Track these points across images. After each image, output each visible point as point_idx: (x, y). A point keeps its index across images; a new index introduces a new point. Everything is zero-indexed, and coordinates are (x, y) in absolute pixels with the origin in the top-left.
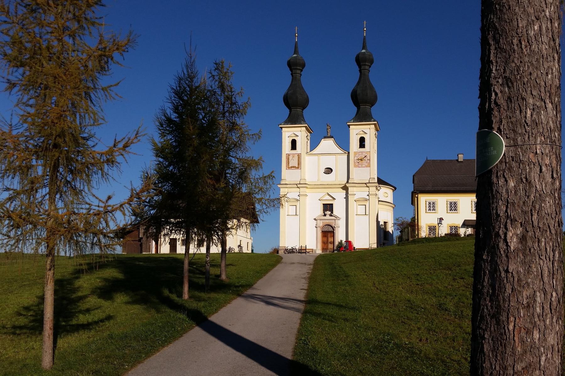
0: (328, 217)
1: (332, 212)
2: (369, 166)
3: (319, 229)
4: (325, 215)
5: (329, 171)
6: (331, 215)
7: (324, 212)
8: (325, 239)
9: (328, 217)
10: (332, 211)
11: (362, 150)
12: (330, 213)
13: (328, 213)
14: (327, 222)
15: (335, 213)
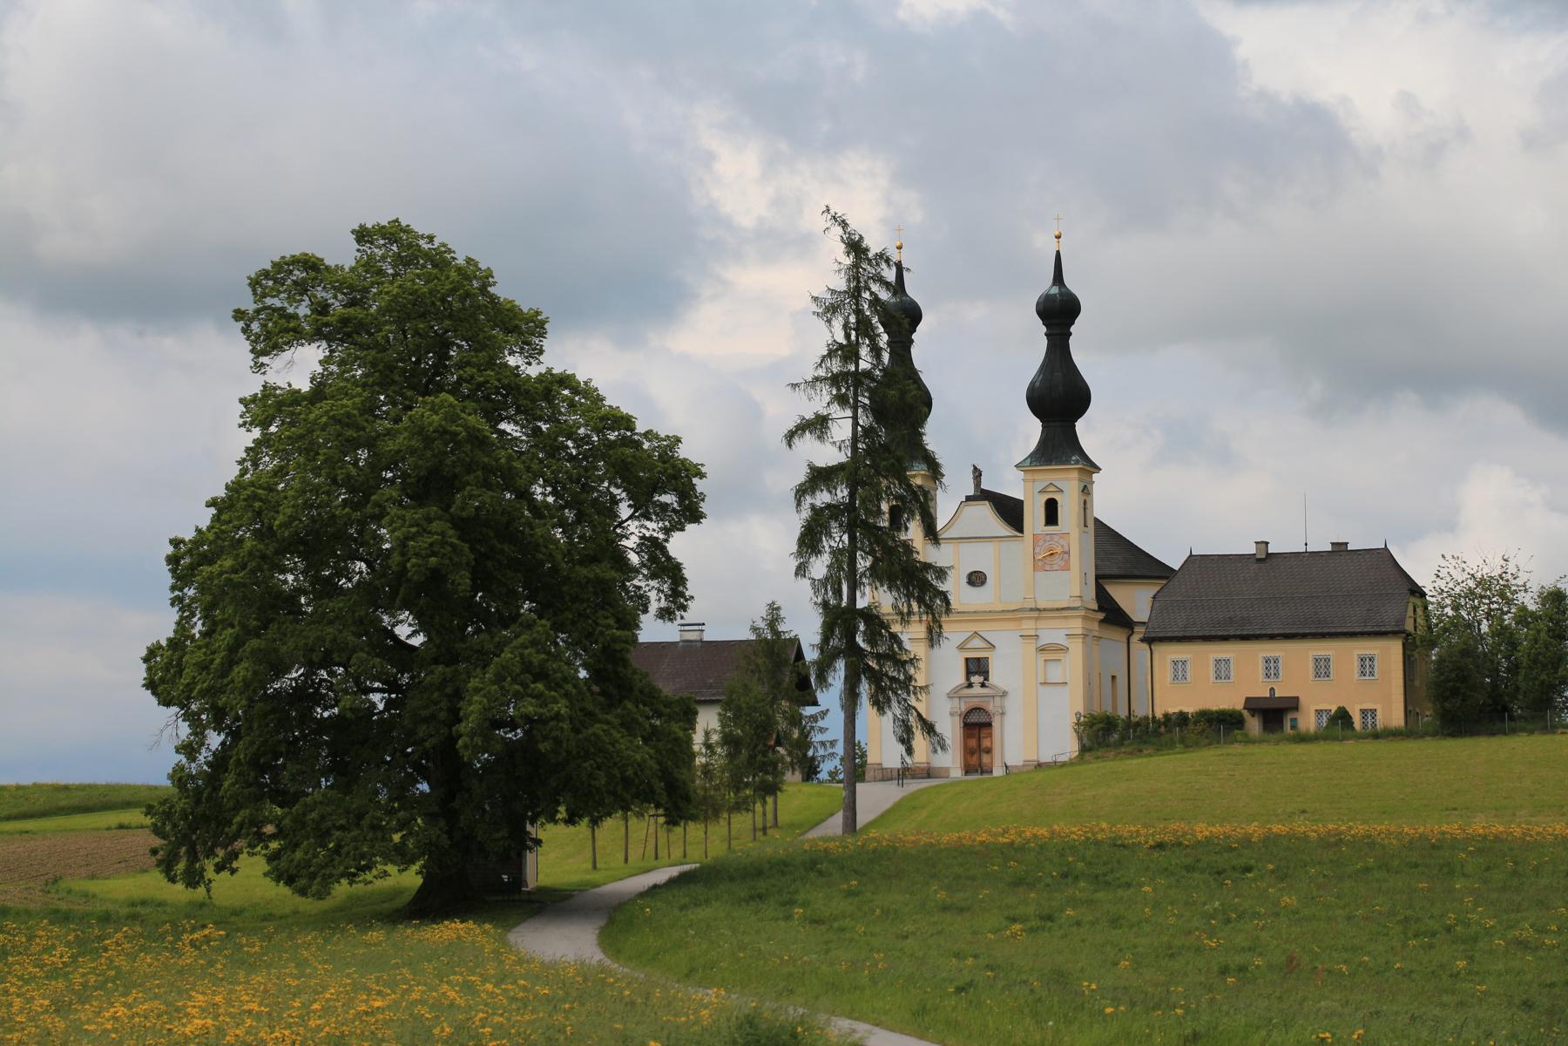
0: (977, 690)
1: (986, 679)
2: (1067, 568)
3: (957, 719)
4: (970, 685)
5: (976, 579)
6: (983, 685)
7: (968, 679)
8: (973, 743)
9: (977, 690)
10: (985, 673)
11: (1051, 529)
12: (981, 679)
13: (976, 679)
14: (975, 703)
15: (994, 678)
